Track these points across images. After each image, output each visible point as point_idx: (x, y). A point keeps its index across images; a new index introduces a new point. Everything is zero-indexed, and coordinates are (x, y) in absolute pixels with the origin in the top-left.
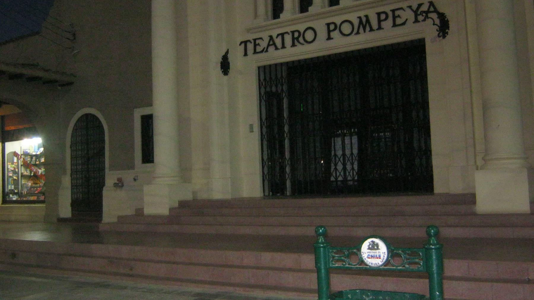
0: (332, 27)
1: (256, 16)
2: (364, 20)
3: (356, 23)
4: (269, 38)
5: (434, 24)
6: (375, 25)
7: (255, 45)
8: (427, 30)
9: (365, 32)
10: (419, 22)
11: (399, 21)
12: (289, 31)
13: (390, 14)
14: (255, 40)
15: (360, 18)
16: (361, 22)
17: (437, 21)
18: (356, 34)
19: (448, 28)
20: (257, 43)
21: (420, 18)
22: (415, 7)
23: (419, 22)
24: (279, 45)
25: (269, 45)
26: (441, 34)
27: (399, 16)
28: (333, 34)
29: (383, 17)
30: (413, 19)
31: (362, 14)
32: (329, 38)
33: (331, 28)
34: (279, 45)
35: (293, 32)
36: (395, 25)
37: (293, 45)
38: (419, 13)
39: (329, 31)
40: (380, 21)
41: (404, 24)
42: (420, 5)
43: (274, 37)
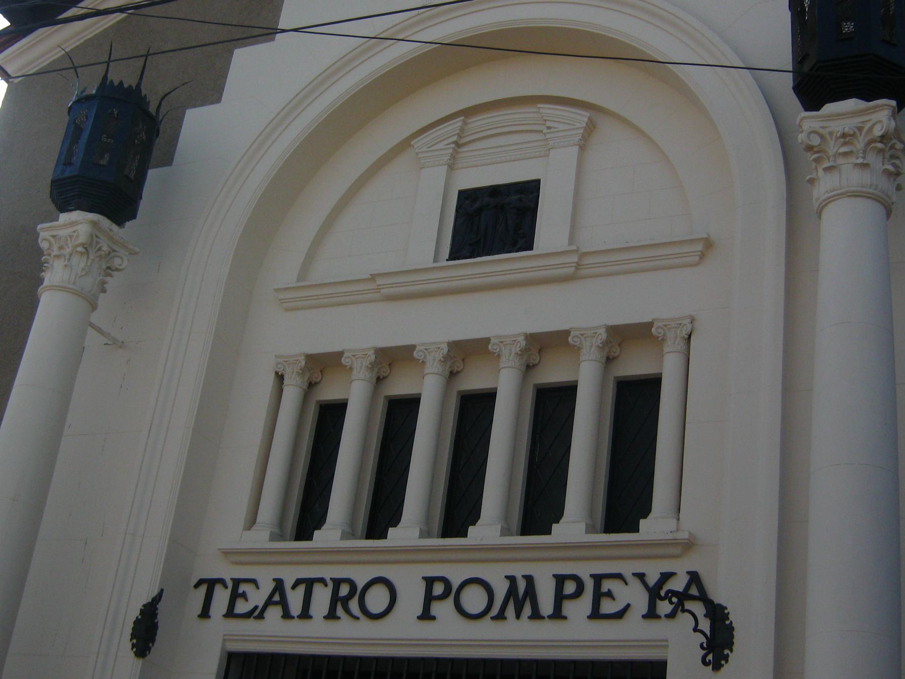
0: (438, 589)
1: (252, 522)
2: (522, 586)
3: (501, 589)
4: (272, 585)
5: (695, 630)
6: (546, 605)
7: (235, 596)
8: (678, 642)
9: (518, 616)
10: (659, 617)
11: (607, 607)
12: (328, 577)
13: (589, 585)
14: (237, 582)
15: (512, 579)
16: (512, 591)
17: (705, 625)
18: (493, 618)
19: (730, 645)
20: (240, 591)
21: (664, 607)
22: (652, 580)
23: (659, 617)
24: (296, 607)
25: (269, 602)
26: (710, 657)
27: (609, 594)
28: (437, 608)
29: (570, 588)
30: (645, 611)
31: (519, 570)
32: (426, 615)
33: (436, 591)
34: (296, 607)
35: (337, 583)
36: (596, 614)
37: (331, 615)
38: (663, 593)
39: (429, 599)
40: (560, 598)
41: (619, 615)
42: (666, 577)
43: (288, 585)
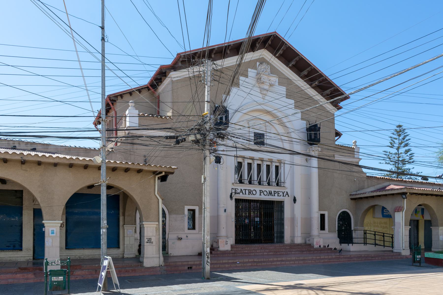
3: (268, 192)
6: (273, 195)
24: (244, 193)
31: (270, 190)
32: (260, 195)
33: (261, 192)
34: (244, 193)
37: (249, 194)
40: (274, 194)
